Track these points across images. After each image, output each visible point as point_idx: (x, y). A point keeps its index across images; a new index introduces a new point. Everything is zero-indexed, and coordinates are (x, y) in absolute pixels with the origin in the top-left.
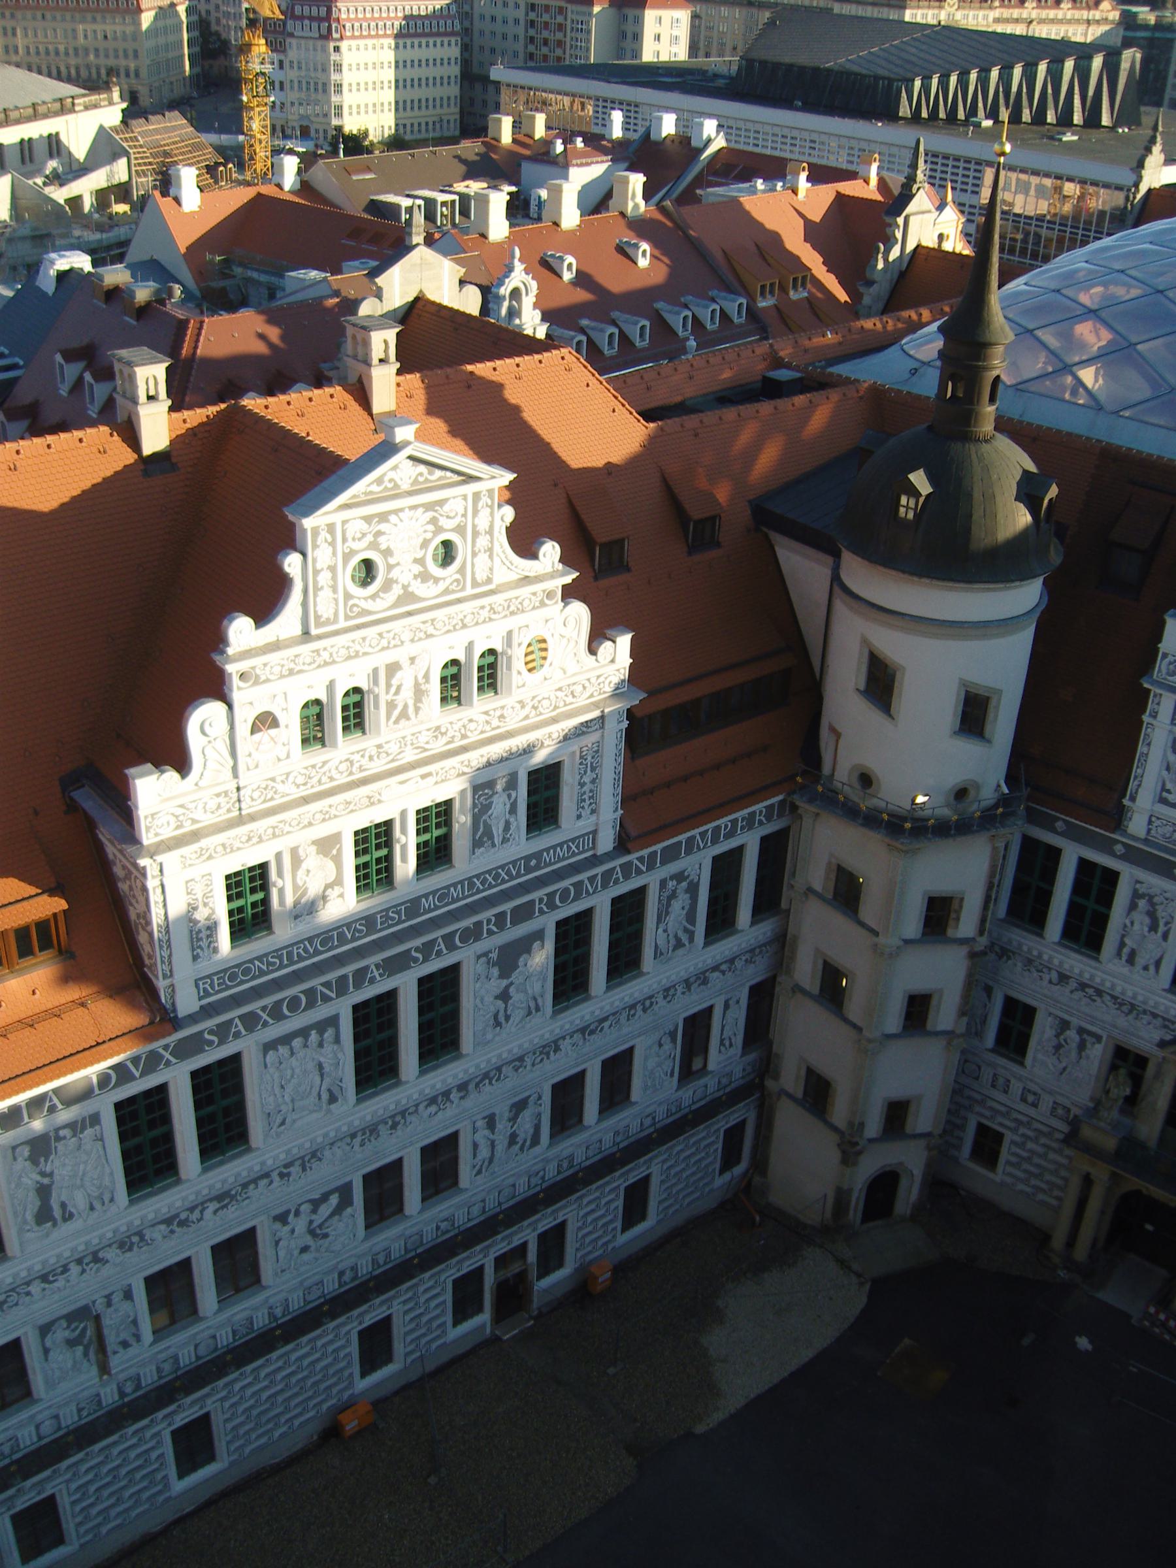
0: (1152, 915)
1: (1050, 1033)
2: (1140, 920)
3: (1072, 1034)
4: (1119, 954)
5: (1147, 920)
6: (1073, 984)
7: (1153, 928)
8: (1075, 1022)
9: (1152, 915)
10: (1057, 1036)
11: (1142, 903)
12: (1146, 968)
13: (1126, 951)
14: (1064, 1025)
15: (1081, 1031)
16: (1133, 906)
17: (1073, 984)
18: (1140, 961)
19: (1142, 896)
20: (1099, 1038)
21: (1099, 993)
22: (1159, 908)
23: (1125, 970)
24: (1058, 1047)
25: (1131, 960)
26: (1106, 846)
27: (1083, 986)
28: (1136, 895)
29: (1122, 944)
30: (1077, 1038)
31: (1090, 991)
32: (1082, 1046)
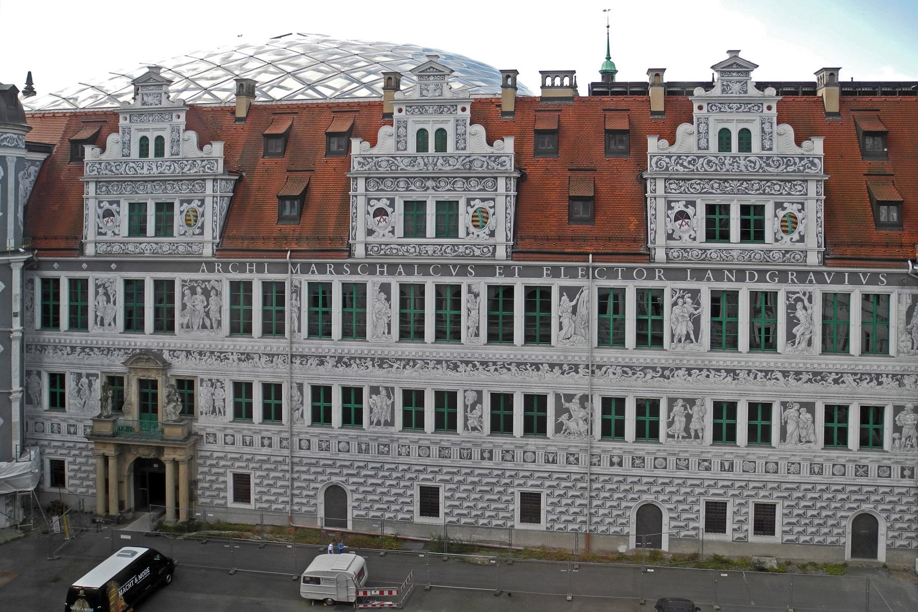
0: (106, 294)
1: (73, 384)
2: (102, 298)
3: (84, 380)
4: (96, 323)
5: (105, 298)
6: (78, 350)
7: (108, 301)
8: (84, 372)
9: (106, 294)
10: (77, 385)
11: (101, 290)
12: (110, 325)
13: (99, 319)
14: (79, 376)
15: (88, 375)
16: (97, 293)
17: (78, 350)
18: (106, 322)
19: (100, 286)
20: (96, 376)
21: (91, 349)
22: (109, 289)
23: (101, 331)
24: (79, 391)
25: (102, 324)
26: (77, 266)
27: (83, 349)
28: (97, 286)
29: (96, 316)
30: (87, 381)
31: (87, 350)
32: (90, 385)
